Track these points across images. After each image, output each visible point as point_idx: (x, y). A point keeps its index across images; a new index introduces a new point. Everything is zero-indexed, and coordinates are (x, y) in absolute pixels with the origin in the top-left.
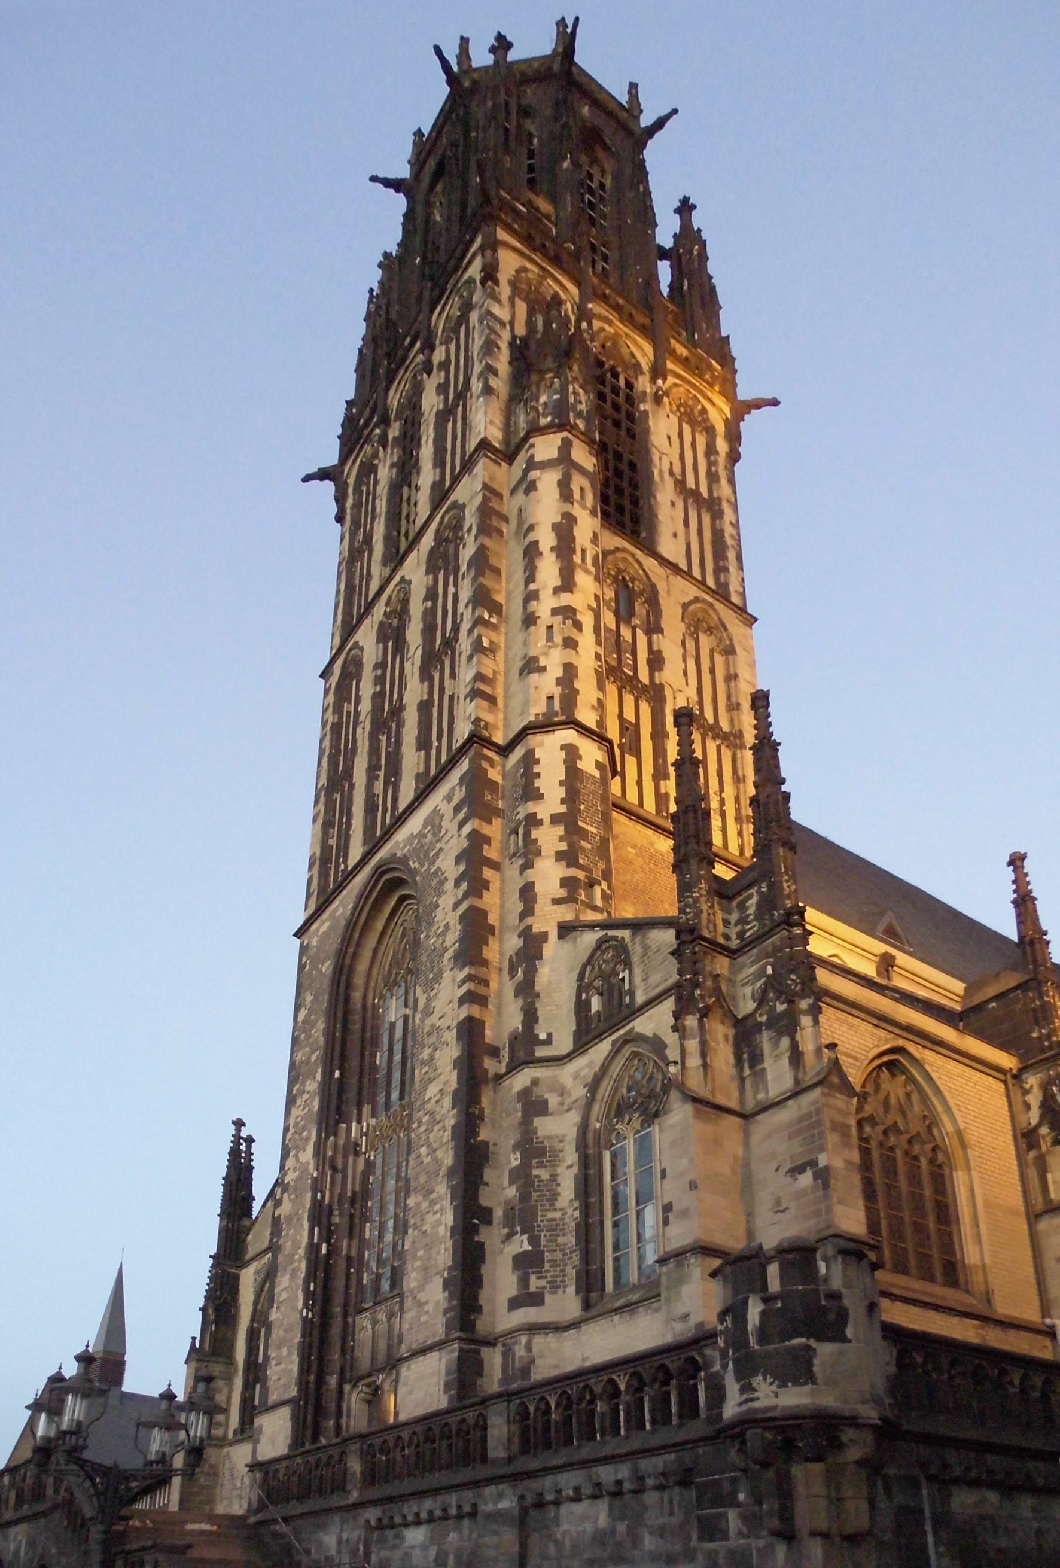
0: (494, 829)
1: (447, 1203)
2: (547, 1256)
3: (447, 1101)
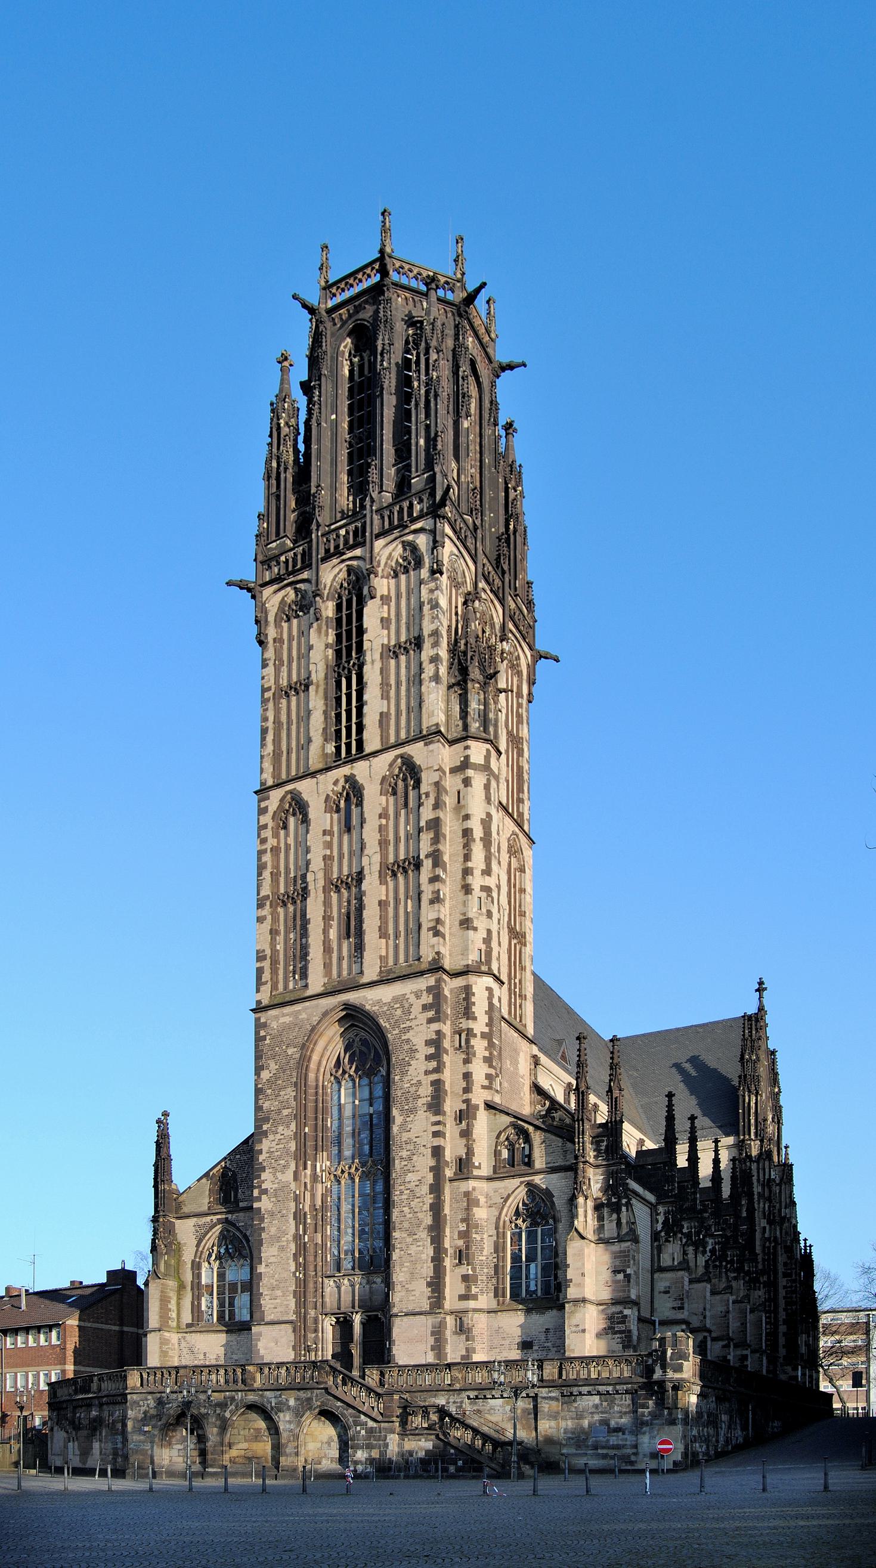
0: (447, 1028)
3: (425, 1189)
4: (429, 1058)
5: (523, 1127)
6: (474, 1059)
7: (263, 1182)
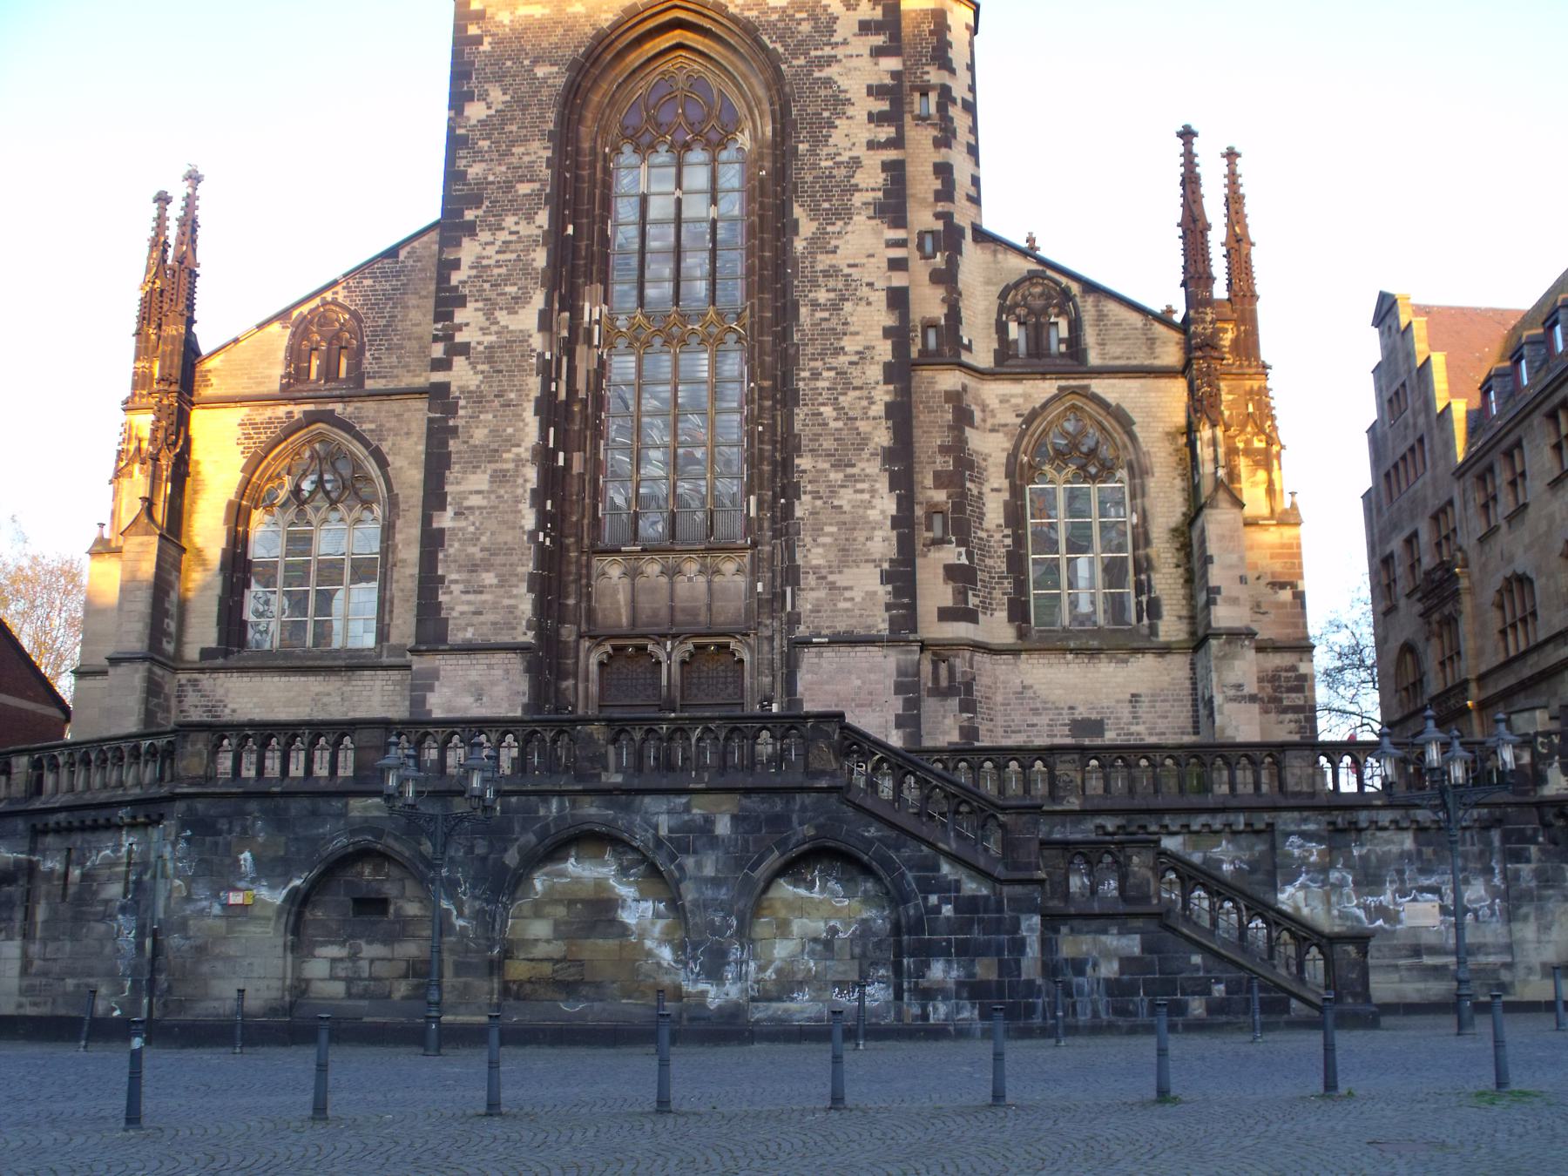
1: (883, 485)
2: (980, 575)
3: (875, 372)
4: (875, 118)
5: (1057, 283)
6: (953, 142)
7: (459, 328)
